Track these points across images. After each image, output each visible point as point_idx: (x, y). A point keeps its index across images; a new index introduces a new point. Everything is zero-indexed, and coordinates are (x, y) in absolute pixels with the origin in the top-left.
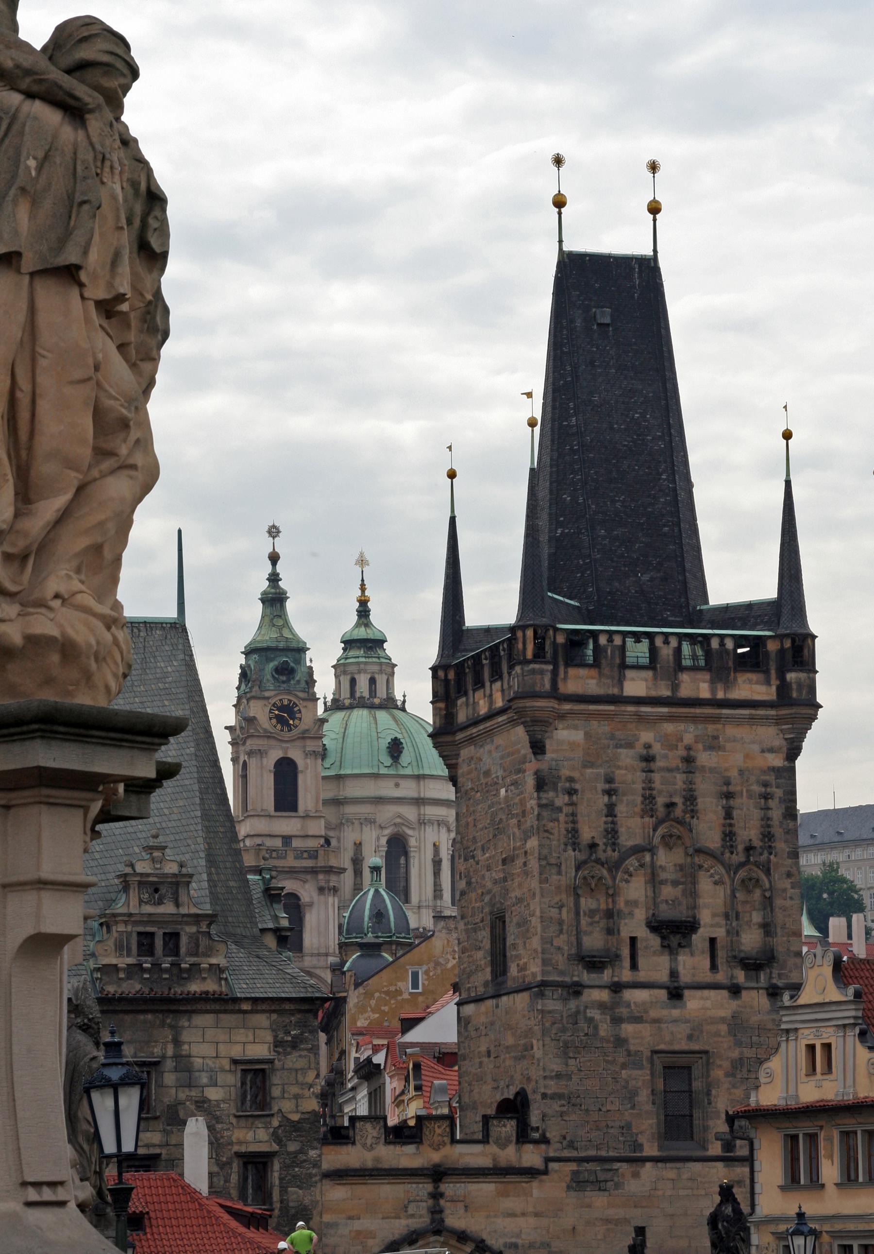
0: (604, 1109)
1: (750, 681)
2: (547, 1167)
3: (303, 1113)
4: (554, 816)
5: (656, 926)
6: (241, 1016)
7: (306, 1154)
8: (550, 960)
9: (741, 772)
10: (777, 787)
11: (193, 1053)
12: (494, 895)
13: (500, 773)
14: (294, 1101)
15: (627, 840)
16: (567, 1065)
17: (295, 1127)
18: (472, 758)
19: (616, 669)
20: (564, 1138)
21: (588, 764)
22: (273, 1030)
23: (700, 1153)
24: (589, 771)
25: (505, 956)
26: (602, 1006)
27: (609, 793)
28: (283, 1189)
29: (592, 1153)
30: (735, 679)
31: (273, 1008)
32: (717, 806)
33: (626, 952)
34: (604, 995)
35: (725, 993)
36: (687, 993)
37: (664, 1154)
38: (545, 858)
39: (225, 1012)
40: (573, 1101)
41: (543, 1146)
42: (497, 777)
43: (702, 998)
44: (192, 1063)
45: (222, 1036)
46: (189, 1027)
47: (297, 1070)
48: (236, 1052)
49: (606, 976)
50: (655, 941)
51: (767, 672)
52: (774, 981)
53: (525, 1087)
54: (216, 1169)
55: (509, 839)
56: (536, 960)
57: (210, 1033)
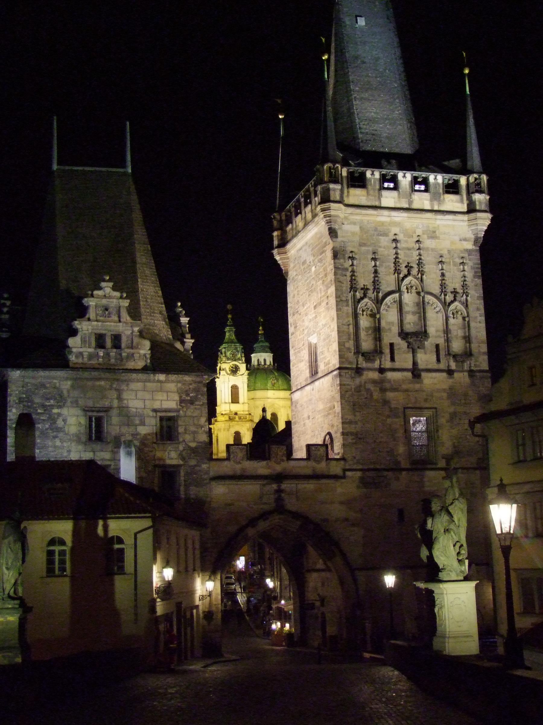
0: (377, 441)
1: (452, 201)
2: (344, 473)
3: (198, 442)
4: (344, 273)
5: (404, 335)
6: (159, 384)
7: (200, 466)
8: (344, 355)
9: (449, 252)
10: (470, 260)
11: (130, 405)
12: (310, 328)
13: (312, 258)
14: (192, 435)
15: (385, 287)
16: (355, 416)
17: (194, 451)
18: (296, 258)
19: (377, 192)
20: (355, 458)
21: (361, 245)
22: (179, 394)
23: (434, 466)
24: (363, 248)
25: (316, 361)
26: (374, 382)
27: (374, 259)
28: (187, 486)
29: (372, 467)
30: (444, 199)
31: (179, 379)
32: (437, 269)
33: (387, 351)
34: (375, 375)
35: (445, 374)
36: (423, 374)
37: (414, 467)
38: (340, 297)
39: (149, 381)
40: (359, 436)
41: (342, 462)
42: (310, 262)
43: (431, 378)
44: (129, 412)
45: (147, 396)
46: (127, 390)
47: (194, 417)
48: (157, 405)
49: (377, 364)
50: (403, 344)
51: (462, 195)
52: (472, 368)
53: (331, 431)
54: (144, 475)
55: (318, 293)
56: (335, 356)
57: (140, 394)
